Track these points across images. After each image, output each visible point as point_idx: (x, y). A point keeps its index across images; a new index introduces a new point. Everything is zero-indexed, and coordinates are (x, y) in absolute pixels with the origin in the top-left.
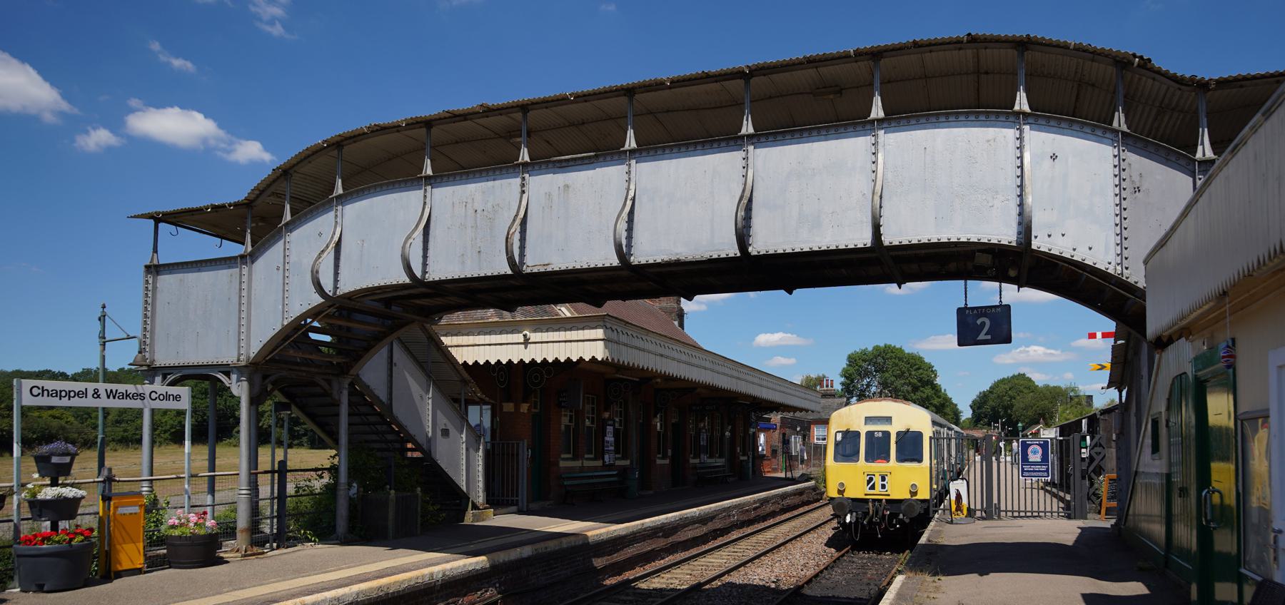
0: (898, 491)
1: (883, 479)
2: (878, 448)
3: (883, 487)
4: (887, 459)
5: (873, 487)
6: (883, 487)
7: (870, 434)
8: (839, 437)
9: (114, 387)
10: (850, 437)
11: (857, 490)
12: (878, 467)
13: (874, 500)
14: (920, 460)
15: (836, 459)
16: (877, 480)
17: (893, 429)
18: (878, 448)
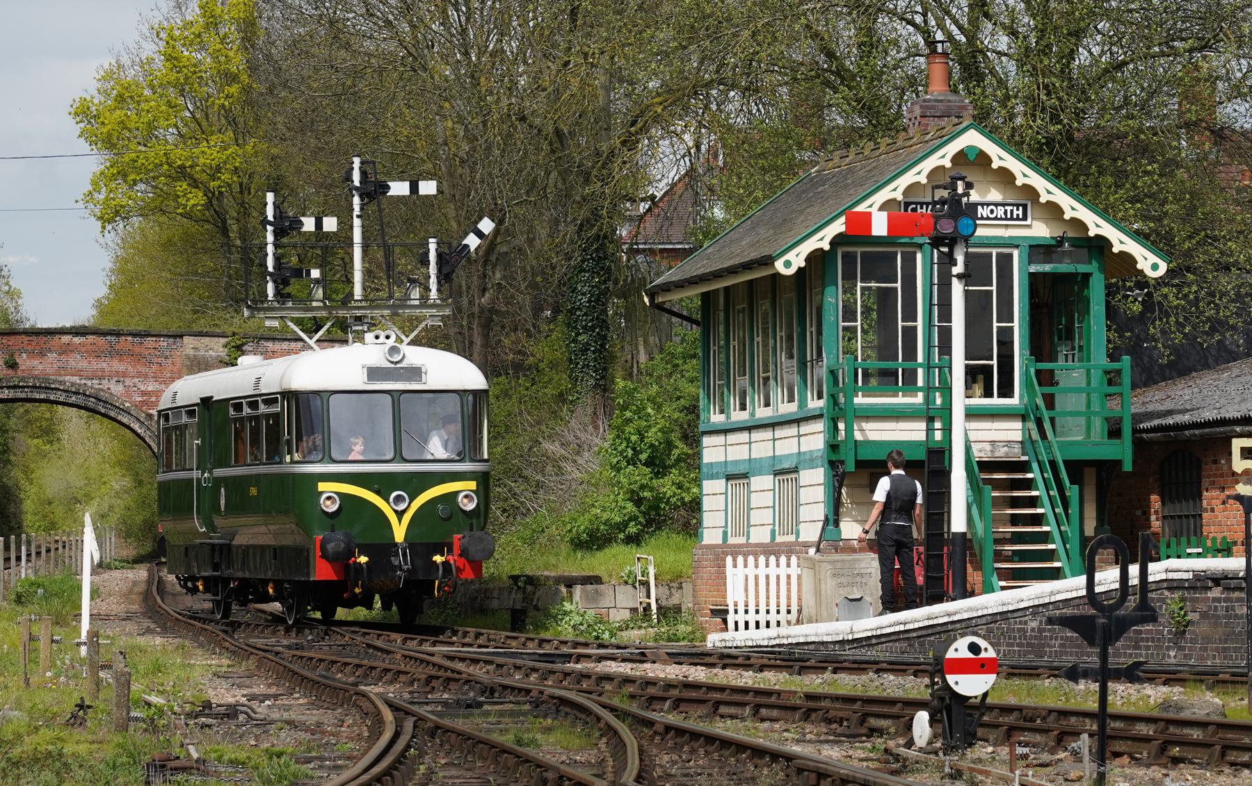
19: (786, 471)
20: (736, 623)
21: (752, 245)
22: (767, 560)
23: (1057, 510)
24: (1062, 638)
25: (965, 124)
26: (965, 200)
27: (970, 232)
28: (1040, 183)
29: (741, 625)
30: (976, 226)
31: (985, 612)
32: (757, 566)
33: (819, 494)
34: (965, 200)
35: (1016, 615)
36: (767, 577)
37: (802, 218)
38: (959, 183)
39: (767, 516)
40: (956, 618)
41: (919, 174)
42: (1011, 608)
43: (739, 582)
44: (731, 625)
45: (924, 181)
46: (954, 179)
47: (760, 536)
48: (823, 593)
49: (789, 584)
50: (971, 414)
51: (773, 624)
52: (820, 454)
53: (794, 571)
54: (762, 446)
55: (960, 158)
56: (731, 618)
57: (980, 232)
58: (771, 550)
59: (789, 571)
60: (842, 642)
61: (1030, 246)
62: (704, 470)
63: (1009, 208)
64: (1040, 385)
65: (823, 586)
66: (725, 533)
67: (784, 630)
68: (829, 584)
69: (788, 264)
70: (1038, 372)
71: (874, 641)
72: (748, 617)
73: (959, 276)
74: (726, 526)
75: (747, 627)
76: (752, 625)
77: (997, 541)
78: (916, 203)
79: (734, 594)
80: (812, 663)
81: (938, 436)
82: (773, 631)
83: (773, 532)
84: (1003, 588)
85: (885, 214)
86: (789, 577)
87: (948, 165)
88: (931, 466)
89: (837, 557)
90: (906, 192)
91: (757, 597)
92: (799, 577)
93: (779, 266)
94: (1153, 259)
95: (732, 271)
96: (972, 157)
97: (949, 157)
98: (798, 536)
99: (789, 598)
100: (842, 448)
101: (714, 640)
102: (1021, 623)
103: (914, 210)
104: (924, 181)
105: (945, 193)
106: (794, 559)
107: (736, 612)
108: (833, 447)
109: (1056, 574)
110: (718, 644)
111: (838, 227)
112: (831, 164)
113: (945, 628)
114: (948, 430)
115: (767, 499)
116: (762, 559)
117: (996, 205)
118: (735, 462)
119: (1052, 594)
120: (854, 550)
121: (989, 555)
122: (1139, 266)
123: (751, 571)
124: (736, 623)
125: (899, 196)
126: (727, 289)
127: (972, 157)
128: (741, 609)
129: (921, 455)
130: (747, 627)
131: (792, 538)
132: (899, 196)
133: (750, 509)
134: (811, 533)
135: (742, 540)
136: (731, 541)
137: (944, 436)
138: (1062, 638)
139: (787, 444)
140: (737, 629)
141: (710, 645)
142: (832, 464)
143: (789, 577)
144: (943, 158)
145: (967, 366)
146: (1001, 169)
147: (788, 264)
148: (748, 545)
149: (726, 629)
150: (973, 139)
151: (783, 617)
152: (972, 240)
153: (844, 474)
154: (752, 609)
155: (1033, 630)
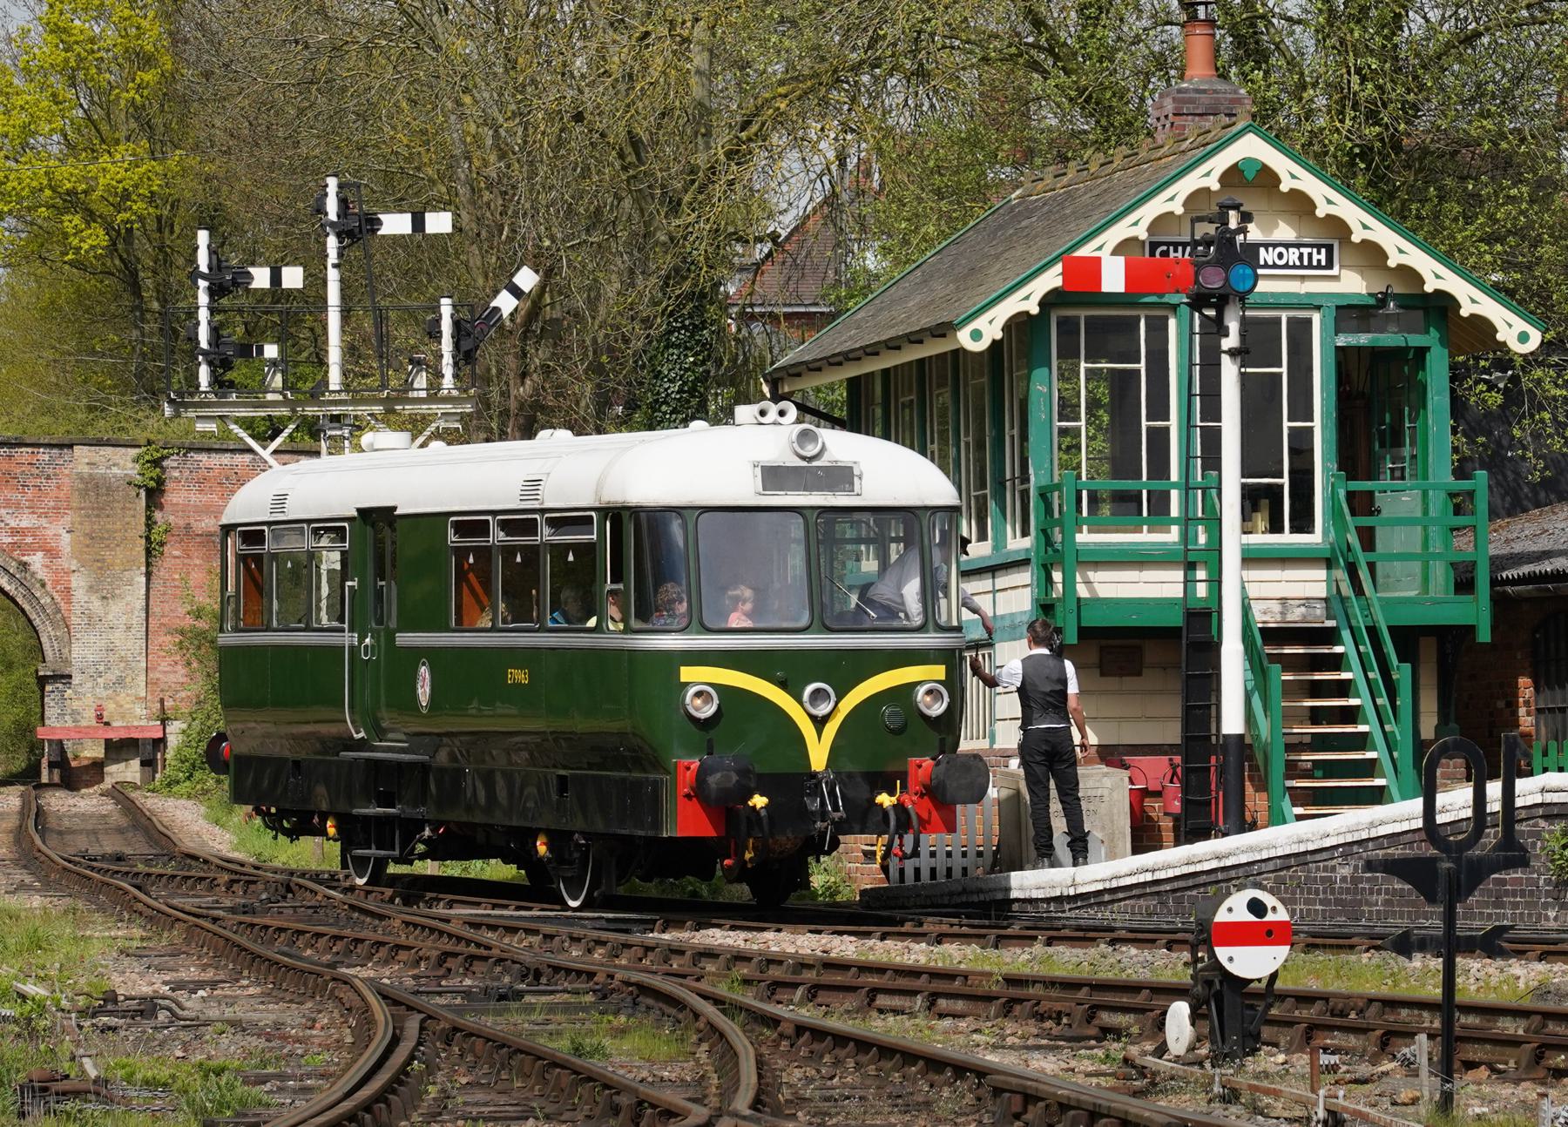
21: (922, 307)
24: (1387, 892)
25: (1239, 126)
26: (1240, 238)
30: (1257, 277)
31: (1273, 854)
34: (1240, 238)
35: (1318, 857)
37: (998, 266)
38: (1232, 213)
40: (1229, 862)
41: (1171, 201)
42: (1311, 847)
45: (1179, 210)
46: (1225, 208)
50: (1252, 559)
52: (1025, 618)
55: (1232, 176)
57: (1262, 286)
60: (1059, 900)
61: (1338, 307)
63: (1306, 251)
64: (1353, 514)
69: (977, 335)
70: (1351, 496)
71: (1107, 898)
73: (1232, 353)
77: (1290, 748)
78: (1168, 244)
81: (1202, 590)
84: (1299, 818)
85: (1121, 260)
87: (1216, 186)
90: (1154, 226)
93: (964, 338)
94: (1520, 325)
95: (893, 345)
96: (1250, 175)
97: (1216, 174)
98: (993, 741)
100: (1059, 609)
102: (1325, 869)
103: (1165, 254)
104: (1179, 210)
105: (1211, 229)
108: (1046, 608)
109: (1377, 796)
111: (1052, 279)
113: (1212, 878)
114: (1216, 582)
117: (1287, 246)
119: (1372, 825)
122: (1499, 337)
125: (1142, 233)
127: (1250, 175)
129: (1176, 619)
132: (1142, 233)
137: (1210, 590)
138: (1387, 892)
144: (1207, 176)
145: (1244, 486)
147: (977, 335)
150: (1252, 148)
152: (1251, 299)
155: (1344, 879)
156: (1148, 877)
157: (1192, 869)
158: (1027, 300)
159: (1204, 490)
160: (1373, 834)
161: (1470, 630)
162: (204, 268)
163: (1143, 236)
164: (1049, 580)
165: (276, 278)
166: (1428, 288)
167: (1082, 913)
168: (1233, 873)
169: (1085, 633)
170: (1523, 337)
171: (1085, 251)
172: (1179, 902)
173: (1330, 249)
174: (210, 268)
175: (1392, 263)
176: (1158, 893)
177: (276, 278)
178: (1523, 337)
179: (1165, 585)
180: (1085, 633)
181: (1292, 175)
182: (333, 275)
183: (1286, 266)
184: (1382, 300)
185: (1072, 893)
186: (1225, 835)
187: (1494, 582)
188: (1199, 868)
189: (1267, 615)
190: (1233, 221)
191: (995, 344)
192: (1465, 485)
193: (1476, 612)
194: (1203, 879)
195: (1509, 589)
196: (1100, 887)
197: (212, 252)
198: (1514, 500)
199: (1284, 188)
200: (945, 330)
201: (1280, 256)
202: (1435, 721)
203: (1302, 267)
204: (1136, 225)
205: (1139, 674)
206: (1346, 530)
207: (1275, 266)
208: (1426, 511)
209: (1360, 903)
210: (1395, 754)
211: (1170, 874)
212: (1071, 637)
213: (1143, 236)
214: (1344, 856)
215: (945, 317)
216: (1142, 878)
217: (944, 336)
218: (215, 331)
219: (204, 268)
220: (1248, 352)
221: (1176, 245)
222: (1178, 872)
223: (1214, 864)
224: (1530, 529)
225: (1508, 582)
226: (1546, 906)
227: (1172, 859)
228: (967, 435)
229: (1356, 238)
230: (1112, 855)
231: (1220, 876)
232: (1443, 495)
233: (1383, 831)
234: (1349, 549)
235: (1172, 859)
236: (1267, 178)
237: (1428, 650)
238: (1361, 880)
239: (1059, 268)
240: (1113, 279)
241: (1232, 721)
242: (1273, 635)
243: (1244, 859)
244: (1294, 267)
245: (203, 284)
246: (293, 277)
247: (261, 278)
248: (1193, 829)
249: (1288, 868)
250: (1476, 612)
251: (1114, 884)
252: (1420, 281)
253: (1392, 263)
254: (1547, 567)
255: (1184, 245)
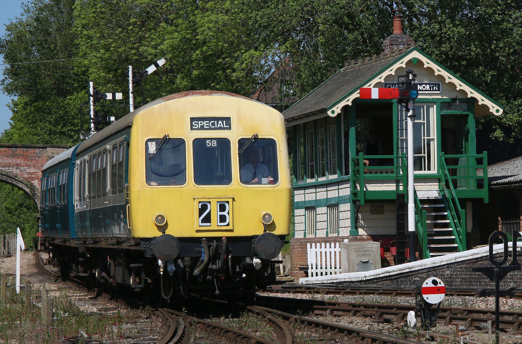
0: (245, 223)
1: (222, 208)
2: (212, 164)
3: (223, 219)
4: (226, 179)
5: (207, 219)
6: (223, 219)
7: (199, 143)
8: (153, 148)
9: (463, 333)
10: (170, 145)
11: (185, 224)
12: (213, 192)
13: (210, 239)
14: (275, 181)
15: (148, 180)
16: (214, 209)
17: (233, 136)
18: (212, 164)
19: (333, 205)
20: (312, 273)
21: (316, 104)
22: (325, 245)
23: (455, 221)
25: (412, 48)
26: (413, 82)
27: (415, 96)
28: (445, 73)
29: (314, 274)
30: (418, 94)
32: (321, 248)
33: (348, 215)
36: (326, 252)
39: (324, 225)
41: (391, 71)
42: (437, 265)
43: (313, 255)
44: (310, 274)
45: (394, 74)
46: (408, 73)
47: (321, 234)
48: (351, 260)
49: (335, 255)
50: (418, 179)
51: (329, 273)
52: (349, 197)
53: (338, 249)
54: (322, 194)
56: (310, 271)
57: (419, 97)
58: (326, 240)
59: (336, 250)
60: (361, 282)
62: (295, 205)
64: (447, 164)
65: (351, 256)
66: (305, 234)
67: (334, 276)
68: (354, 256)
69: (333, 112)
70: (446, 160)
71: (375, 281)
72: (317, 271)
73: (410, 116)
74: (305, 230)
75: (317, 275)
76: (319, 274)
77: (429, 235)
78: (390, 84)
79: (311, 260)
80: (348, 290)
81: (401, 188)
82: (329, 277)
83: (327, 232)
84: (432, 256)
86: (335, 252)
87: (404, 66)
88: (399, 202)
89: (356, 243)
91: (321, 261)
92: (340, 252)
93: (329, 113)
95: (307, 115)
97: (404, 63)
99: (335, 262)
101: (302, 281)
102: (442, 271)
103: (389, 87)
104: (394, 74)
105: (403, 79)
106: (337, 244)
107: (312, 268)
108: (354, 194)
110: (304, 283)
112: (350, 67)
113: (407, 274)
114: (406, 186)
115: (324, 217)
116: (323, 244)
118: (309, 202)
119: (456, 258)
120: (364, 240)
121: (425, 242)
123: (318, 250)
124: (312, 273)
126: (304, 124)
127: (415, 63)
128: (314, 267)
129: (394, 197)
130: (317, 275)
131: (336, 235)
133: (316, 222)
134: (345, 232)
135: (313, 236)
136: (308, 236)
137: (404, 188)
139: (333, 193)
140: (312, 276)
141: (300, 283)
142: (354, 202)
143: (335, 252)
144: (402, 63)
145: (414, 156)
146: (428, 68)
147: (333, 112)
148: (316, 238)
149: (307, 276)
150: (416, 55)
151: (333, 270)
152: (416, 100)
153: (359, 206)
154: (319, 267)
155: (448, 275)
156: (388, 274)
157: (401, 272)
158: (348, 101)
159: (402, 158)
160: (457, 261)
161: (482, 199)
162: (92, 93)
163: (383, 81)
164: (356, 187)
165: (114, 96)
166: (469, 96)
167: (368, 285)
168: (414, 273)
169: (366, 201)
170: (498, 111)
171: (365, 87)
172: (397, 282)
173: (439, 85)
174: (94, 93)
175: (458, 89)
176: (391, 280)
177: (114, 96)
178: (498, 111)
179: (391, 187)
180: (366, 201)
181: (427, 63)
182: (131, 95)
183: (426, 90)
184: (454, 100)
185: (364, 279)
186: (410, 262)
187: (490, 185)
188: (403, 271)
189: (421, 195)
190: (411, 77)
191: (339, 115)
192: (480, 156)
193: (484, 194)
194: (404, 275)
195: (493, 187)
196: (373, 277)
197: (94, 88)
198: (493, 161)
199: (425, 66)
200: (325, 110)
201: (424, 87)
202: (472, 227)
203: (430, 90)
204: (381, 78)
205: (383, 213)
206: (445, 169)
207: (422, 90)
208: (468, 164)
209: (452, 282)
210: (461, 237)
211: (395, 273)
212: (362, 202)
213: (383, 81)
214: (448, 268)
215: (322, 106)
216: (386, 275)
217: (323, 112)
218: (96, 112)
219: (92, 93)
220: (415, 116)
221: (393, 84)
222: (397, 273)
223: (408, 270)
224: (511, 167)
225: (493, 185)
226: (510, 282)
227: (394, 269)
228: (330, 142)
229: (447, 81)
230: (375, 268)
231: (410, 274)
232: (474, 159)
233: (459, 260)
234: (446, 175)
235: (394, 269)
236: (420, 63)
237: (469, 205)
238: (452, 275)
239: (359, 91)
240: (375, 94)
241: (411, 228)
242: (423, 201)
243: (417, 269)
244: (428, 91)
245: (92, 98)
246: (119, 96)
247: (109, 96)
248: (400, 260)
249: (431, 271)
250: (484, 194)
251: (377, 276)
252: (466, 94)
253: (458, 89)
254: (506, 180)
255: (395, 84)
